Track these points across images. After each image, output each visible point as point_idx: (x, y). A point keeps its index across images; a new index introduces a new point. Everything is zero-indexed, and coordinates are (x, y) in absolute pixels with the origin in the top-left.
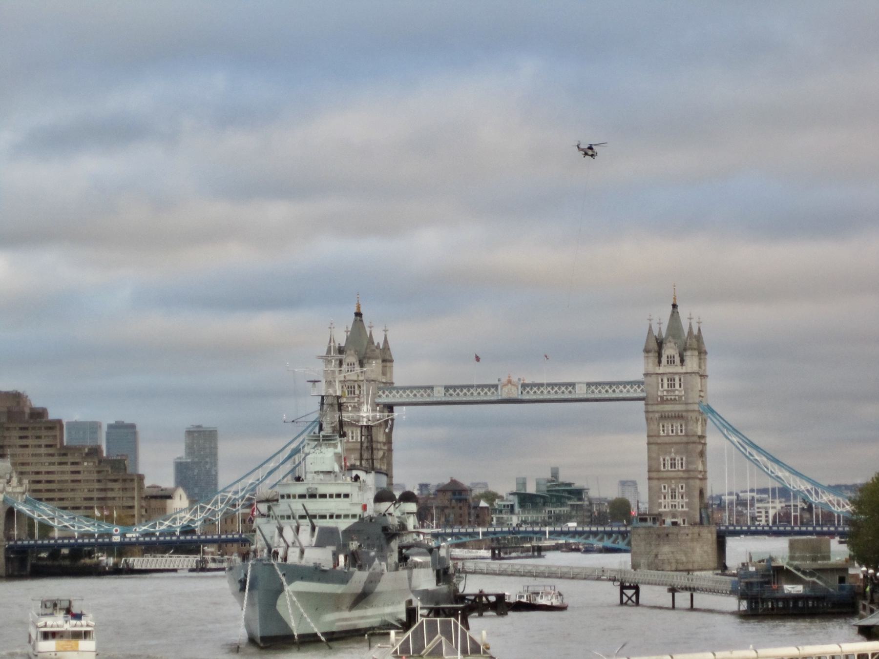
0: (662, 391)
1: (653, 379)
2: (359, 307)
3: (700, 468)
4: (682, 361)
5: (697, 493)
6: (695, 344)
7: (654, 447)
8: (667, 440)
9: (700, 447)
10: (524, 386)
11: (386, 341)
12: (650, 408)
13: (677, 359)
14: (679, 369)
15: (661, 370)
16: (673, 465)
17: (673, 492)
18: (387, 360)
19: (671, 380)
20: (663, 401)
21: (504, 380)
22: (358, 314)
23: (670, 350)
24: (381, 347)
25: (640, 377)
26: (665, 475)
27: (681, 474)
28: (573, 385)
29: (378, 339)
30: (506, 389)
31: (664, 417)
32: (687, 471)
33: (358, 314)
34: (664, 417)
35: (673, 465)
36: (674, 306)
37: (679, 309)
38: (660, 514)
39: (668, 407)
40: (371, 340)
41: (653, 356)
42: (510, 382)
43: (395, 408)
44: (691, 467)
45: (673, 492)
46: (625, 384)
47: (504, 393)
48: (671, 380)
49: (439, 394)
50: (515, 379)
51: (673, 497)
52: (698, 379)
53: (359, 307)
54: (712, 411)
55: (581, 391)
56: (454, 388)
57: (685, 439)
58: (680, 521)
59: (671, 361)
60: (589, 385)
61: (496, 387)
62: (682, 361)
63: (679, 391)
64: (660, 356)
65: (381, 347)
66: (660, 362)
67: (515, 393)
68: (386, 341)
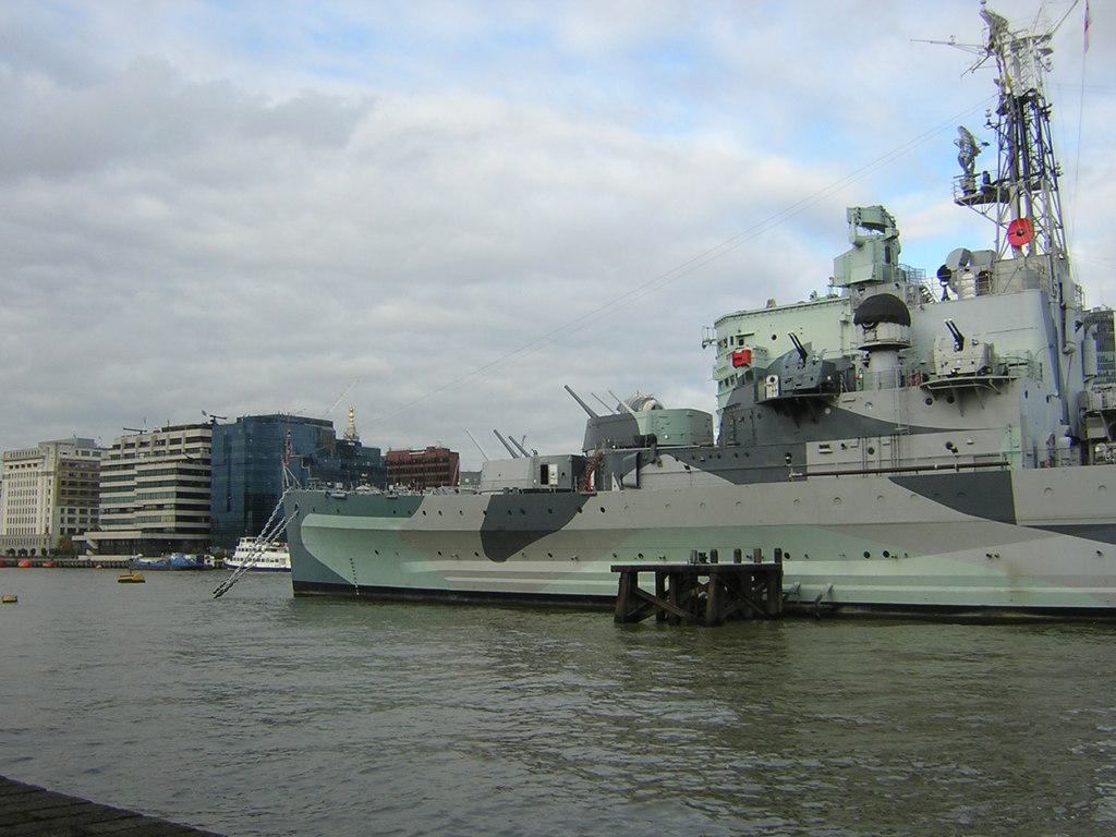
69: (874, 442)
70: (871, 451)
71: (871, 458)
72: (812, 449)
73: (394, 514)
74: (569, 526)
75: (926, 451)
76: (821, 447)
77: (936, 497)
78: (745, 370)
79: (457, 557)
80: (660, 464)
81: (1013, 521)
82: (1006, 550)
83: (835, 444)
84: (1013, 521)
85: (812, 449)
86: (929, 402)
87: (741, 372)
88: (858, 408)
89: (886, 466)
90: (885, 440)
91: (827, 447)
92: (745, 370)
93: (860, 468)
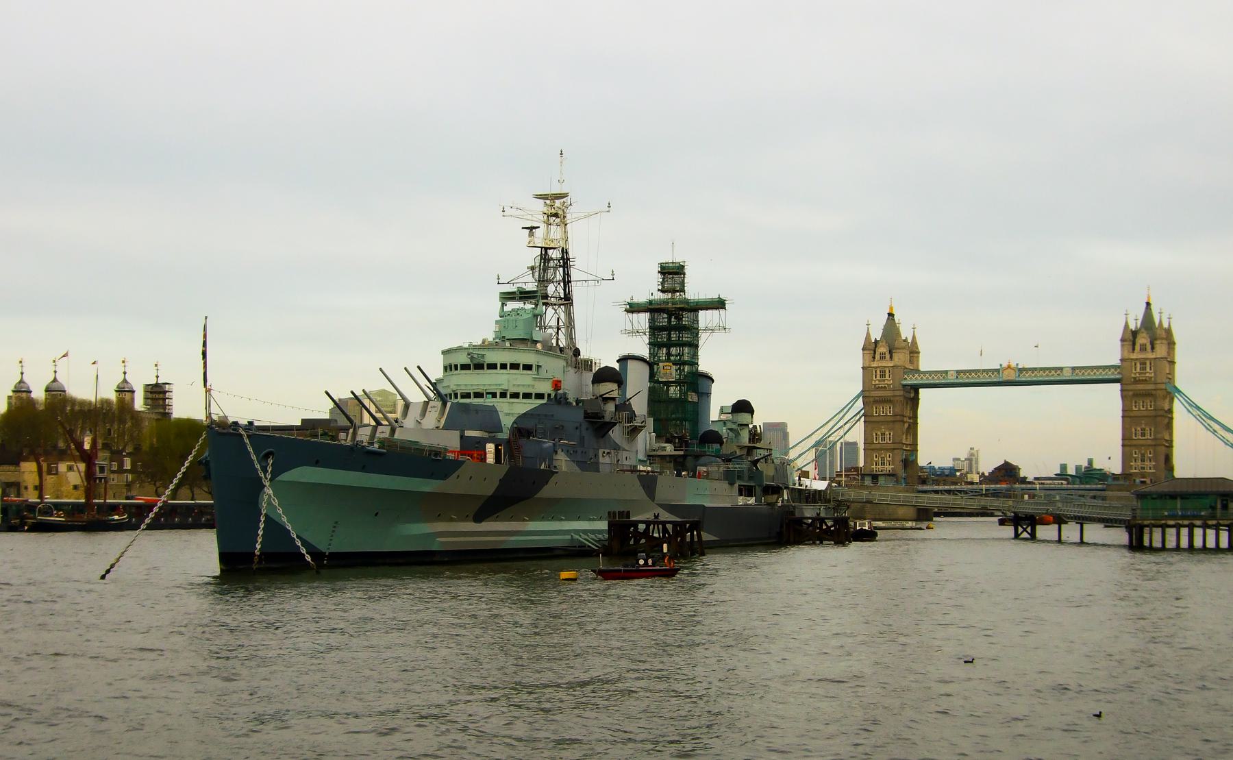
0: (1136, 372)
1: (1127, 364)
2: (891, 308)
3: (1167, 438)
4: (1153, 348)
5: (1162, 458)
6: (1164, 335)
7: (1128, 420)
8: (1138, 414)
9: (1166, 421)
10: (1021, 370)
11: (914, 337)
12: (1126, 387)
13: (1149, 347)
14: (1150, 355)
15: (1134, 356)
16: (1143, 434)
17: (1143, 455)
18: (913, 351)
19: (1143, 363)
20: (1136, 381)
21: (1005, 365)
22: (891, 315)
23: (1143, 339)
24: (910, 340)
25: (1117, 362)
26: (1134, 442)
27: (1149, 442)
28: (1061, 369)
29: (905, 333)
30: (1006, 373)
31: (1138, 395)
32: (1155, 439)
33: (891, 315)
34: (1138, 395)
35: (1143, 434)
36: (1148, 304)
37: (1152, 307)
38: (1131, 475)
39: (1140, 387)
40: (898, 334)
41: (1128, 344)
42: (1009, 367)
43: (921, 390)
44: (1159, 436)
45: (1143, 455)
46: (1105, 368)
47: (1006, 376)
48: (1143, 363)
49: (951, 378)
50: (1013, 365)
51: (1143, 460)
52: (1167, 365)
53: (891, 308)
54: (1179, 392)
55: (1067, 375)
56: (964, 372)
57: (1153, 413)
58: (1148, 481)
59: (1143, 348)
60: (1074, 369)
61: (997, 370)
62: (1153, 348)
63: (1149, 373)
64: (1134, 344)
65: (910, 340)
66: (1134, 349)
67: (1012, 376)
68: (914, 337)
73: (432, 476)
74: (538, 496)
79: (452, 520)
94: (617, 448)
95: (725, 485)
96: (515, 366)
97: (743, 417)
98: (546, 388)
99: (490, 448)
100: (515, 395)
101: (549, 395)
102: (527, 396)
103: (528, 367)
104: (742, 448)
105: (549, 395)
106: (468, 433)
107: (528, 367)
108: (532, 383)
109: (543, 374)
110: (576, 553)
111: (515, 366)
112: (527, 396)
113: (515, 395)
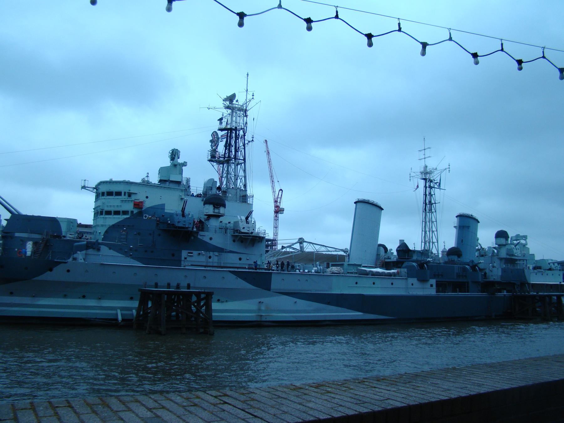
69: (211, 254)
70: (210, 257)
71: (211, 260)
72: (184, 253)
75: (232, 259)
76: (189, 253)
77: (245, 279)
78: (140, 210)
80: (99, 250)
81: (269, 289)
82: (266, 300)
83: (195, 253)
84: (269, 289)
85: (184, 253)
86: (234, 241)
87: (136, 211)
88: (206, 239)
89: (216, 265)
90: (217, 254)
91: (192, 253)
92: (140, 210)
93: (205, 264)
94: (221, 250)
95: (414, 280)
96: (110, 194)
97: (502, 241)
98: (129, 207)
99: (29, 246)
100: (108, 213)
101: (132, 212)
102: (117, 213)
103: (119, 194)
104: (501, 259)
105: (132, 212)
106: (17, 235)
107: (119, 194)
108: (119, 204)
109: (133, 197)
110: (109, 324)
111: (110, 194)
112: (117, 213)
113: (108, 213)
